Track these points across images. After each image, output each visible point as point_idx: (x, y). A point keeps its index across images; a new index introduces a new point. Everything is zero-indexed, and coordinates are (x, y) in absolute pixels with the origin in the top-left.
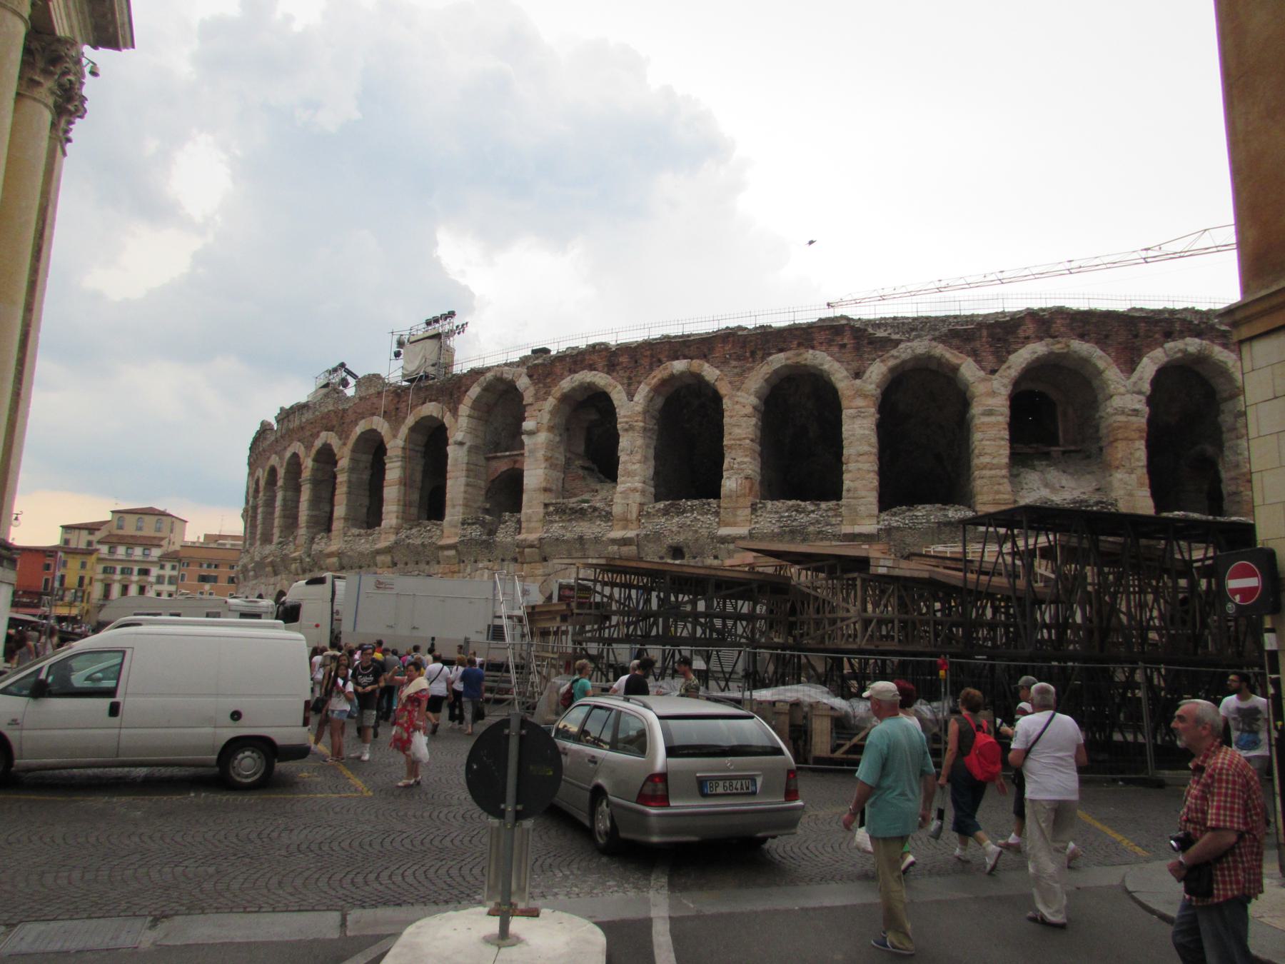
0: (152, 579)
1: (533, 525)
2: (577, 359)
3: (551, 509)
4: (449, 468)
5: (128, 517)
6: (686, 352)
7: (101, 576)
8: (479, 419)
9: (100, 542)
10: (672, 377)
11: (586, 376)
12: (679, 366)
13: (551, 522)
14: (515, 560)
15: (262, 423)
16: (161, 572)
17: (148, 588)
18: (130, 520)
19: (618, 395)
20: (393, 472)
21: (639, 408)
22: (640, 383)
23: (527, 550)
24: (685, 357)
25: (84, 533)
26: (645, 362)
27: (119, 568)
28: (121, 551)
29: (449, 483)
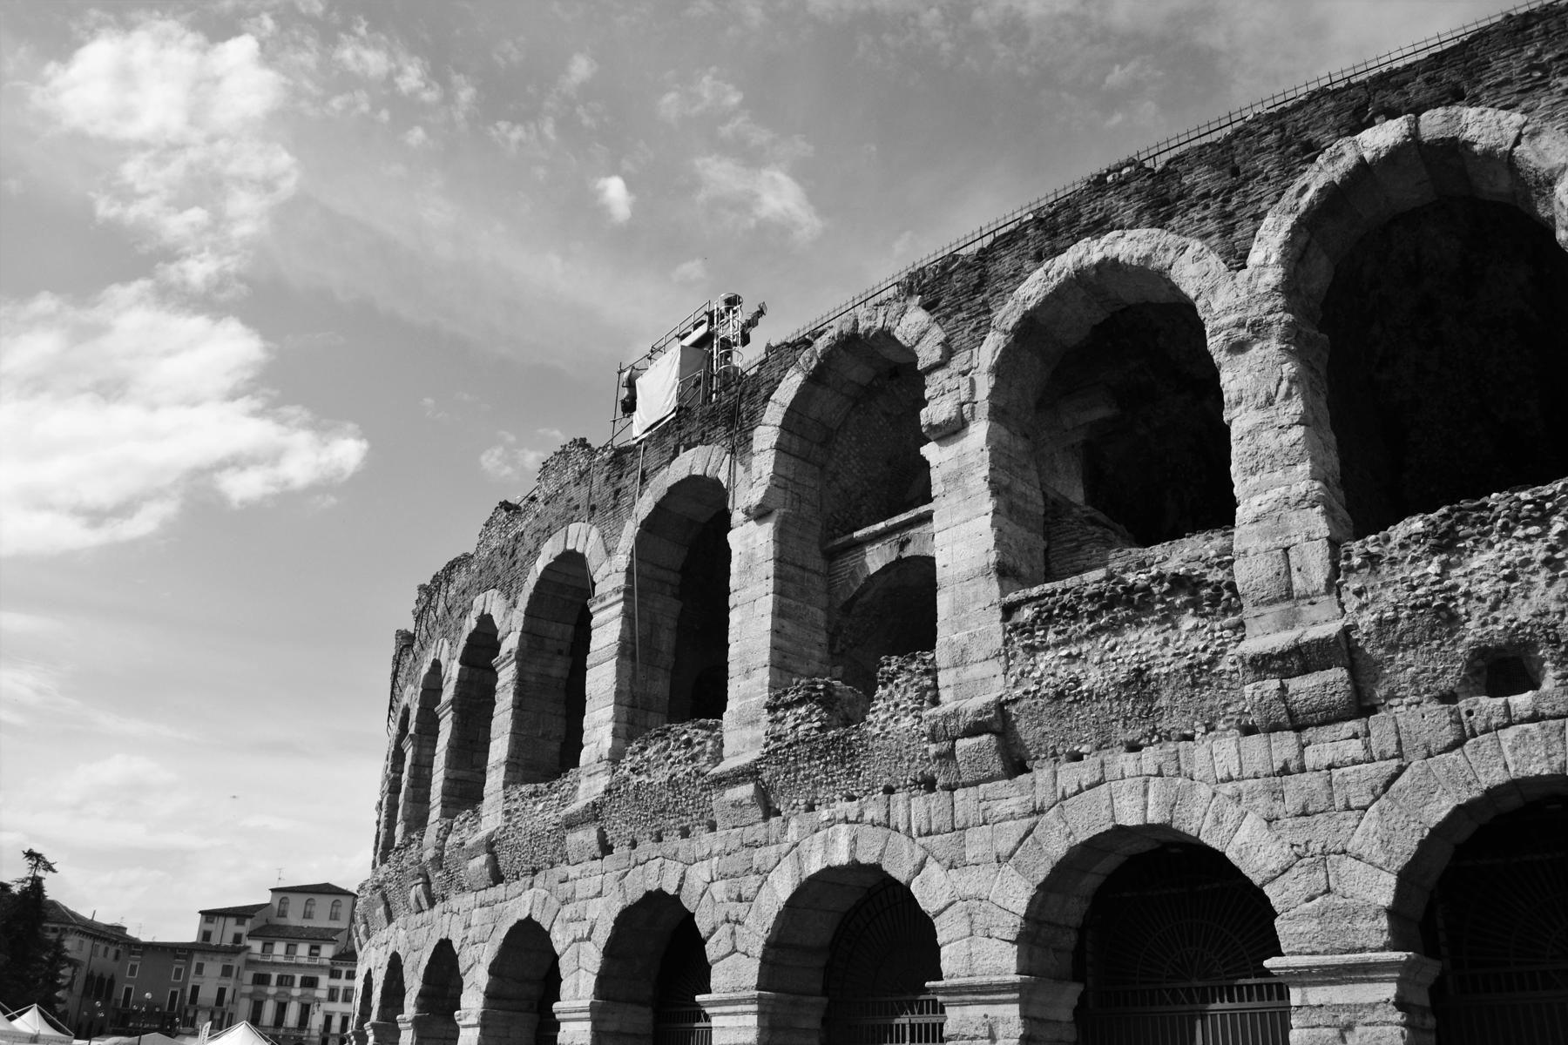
0: (322, 993)
1: (976, 671)
2: (1053, 227)
3: (1027, 613)
4: (734, 582)
5: (292, 897)
6: (1394, 99)
7: (249, 989)
8: (804, 458)
9: (252, 935)
10: (1362, 167)
11: (1088, 252)
12: (1382, 136)
13: (1032, 650)
14: (929, 784)
15: (399, 633)
16: (334, 982)
17: (314, 1008)
18: (298, 902)
19: (1193, 268)
20: (607, 631)
21: (1273, 276)
22: (1258, 217)
23: (961, 744)
24: (1392, 114)
25: (231, 921)
26: (1267, 163)
27: (274, 976)
28: (280, 948)
29: (734, 617)
